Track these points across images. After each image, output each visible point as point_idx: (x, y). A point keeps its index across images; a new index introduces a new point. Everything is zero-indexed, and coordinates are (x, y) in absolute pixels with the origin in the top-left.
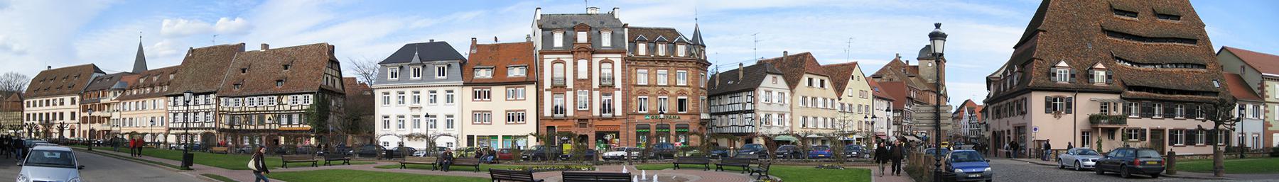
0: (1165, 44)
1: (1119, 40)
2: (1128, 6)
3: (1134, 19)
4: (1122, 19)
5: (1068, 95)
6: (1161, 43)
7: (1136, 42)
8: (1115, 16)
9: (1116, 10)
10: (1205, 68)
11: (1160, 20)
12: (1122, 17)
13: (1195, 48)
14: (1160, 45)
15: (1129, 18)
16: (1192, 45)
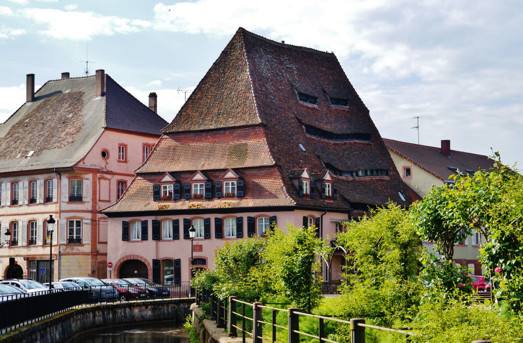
0: (347, 142)
1: (315, 138)
2: (309, 91)
3: (316, 106)
4: (307, 107)
5: (317, 215)
6: (345, 141)
7: (326, 141)
8: (301, 102)
9: (300, 94)
10: (387, 174)
11: (334, 107)
12: (306, 104)
13: (371, 145)
14: (345, 144)
15: (310, 105)
16: (367, 142)
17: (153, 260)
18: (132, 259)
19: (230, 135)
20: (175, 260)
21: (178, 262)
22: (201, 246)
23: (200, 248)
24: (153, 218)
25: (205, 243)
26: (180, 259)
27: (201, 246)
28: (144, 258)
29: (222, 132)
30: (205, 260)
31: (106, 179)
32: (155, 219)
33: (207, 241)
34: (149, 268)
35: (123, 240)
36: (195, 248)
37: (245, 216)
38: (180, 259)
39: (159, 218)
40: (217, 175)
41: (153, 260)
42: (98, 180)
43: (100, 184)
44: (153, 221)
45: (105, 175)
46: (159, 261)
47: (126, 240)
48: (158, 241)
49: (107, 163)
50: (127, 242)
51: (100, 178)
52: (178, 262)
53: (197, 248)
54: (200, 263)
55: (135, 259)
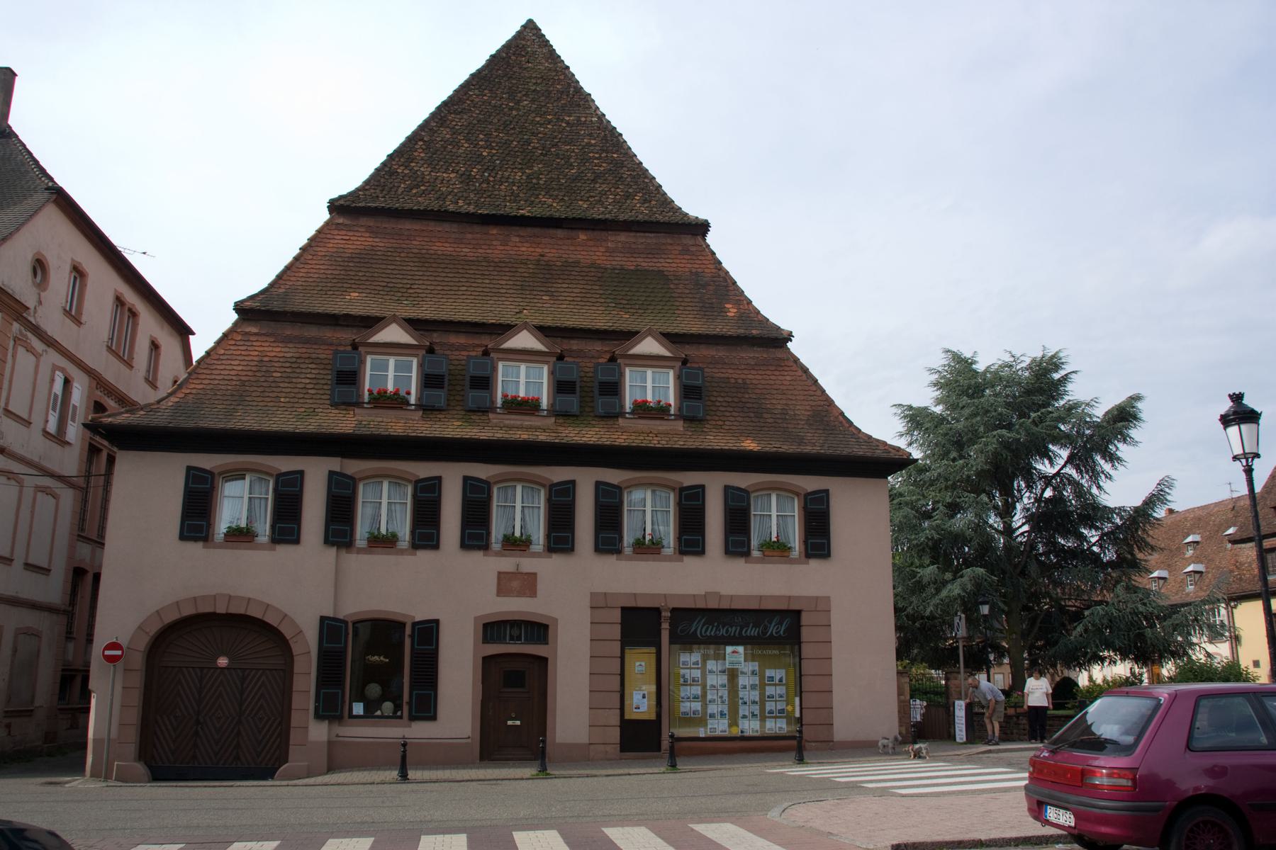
17: (323, 619)
18: (221, 609)
19: (591, 243)
20: (414, 624)
21: (428, 632)
22: (533, 576)
23: (528, 584)
24: (334, 464)
25: (548, 568)
26: (437, 622)
27: (533, 576)
28: (277, 610)
29: (560, 233)
30: (546, 627)
31: (30, 350)
32: (337, 469)
33: (557, 560)
34: (296, 649)
35: (183, 537)
36: (506, 584)
37: (715, 485)
38: (437, 622)
39: (353, 467)
40: (575, 348)
41: (323, 619)
42: (12, 343)
43: (14, 356)
44: (331, 473)
45: (29, 335)
46: (345, 622)
47: (195, 539)
48: (343, 552)
49: (40, 303)
50: (200, 544)
51: (19, 339)
52: (428, 632)
53: (515, 584)
54: (519, 638)
55: (233, 610)
